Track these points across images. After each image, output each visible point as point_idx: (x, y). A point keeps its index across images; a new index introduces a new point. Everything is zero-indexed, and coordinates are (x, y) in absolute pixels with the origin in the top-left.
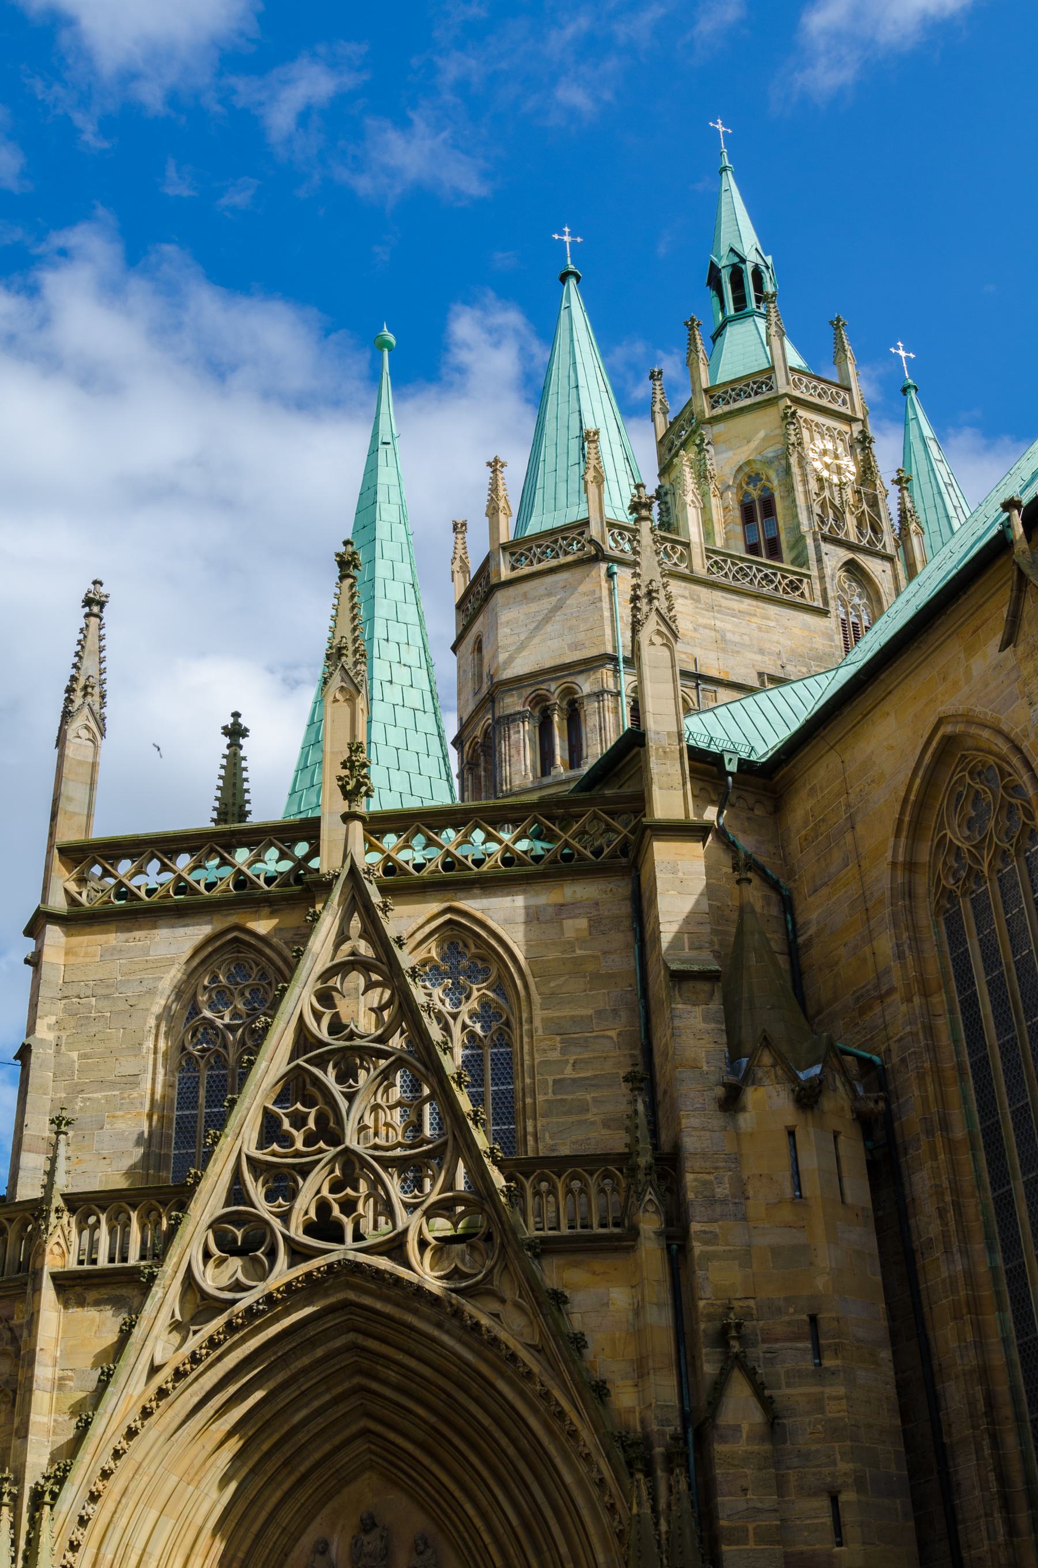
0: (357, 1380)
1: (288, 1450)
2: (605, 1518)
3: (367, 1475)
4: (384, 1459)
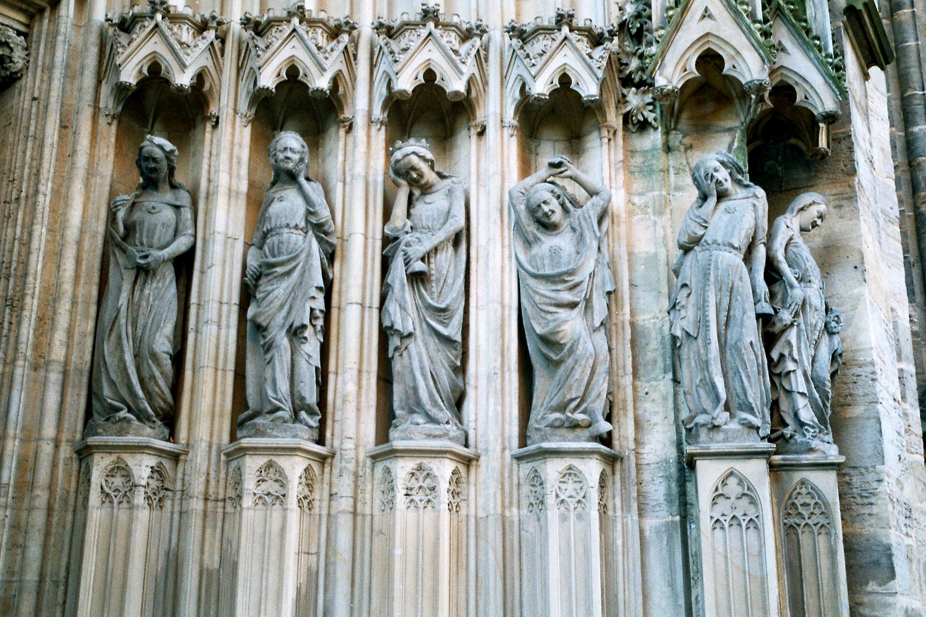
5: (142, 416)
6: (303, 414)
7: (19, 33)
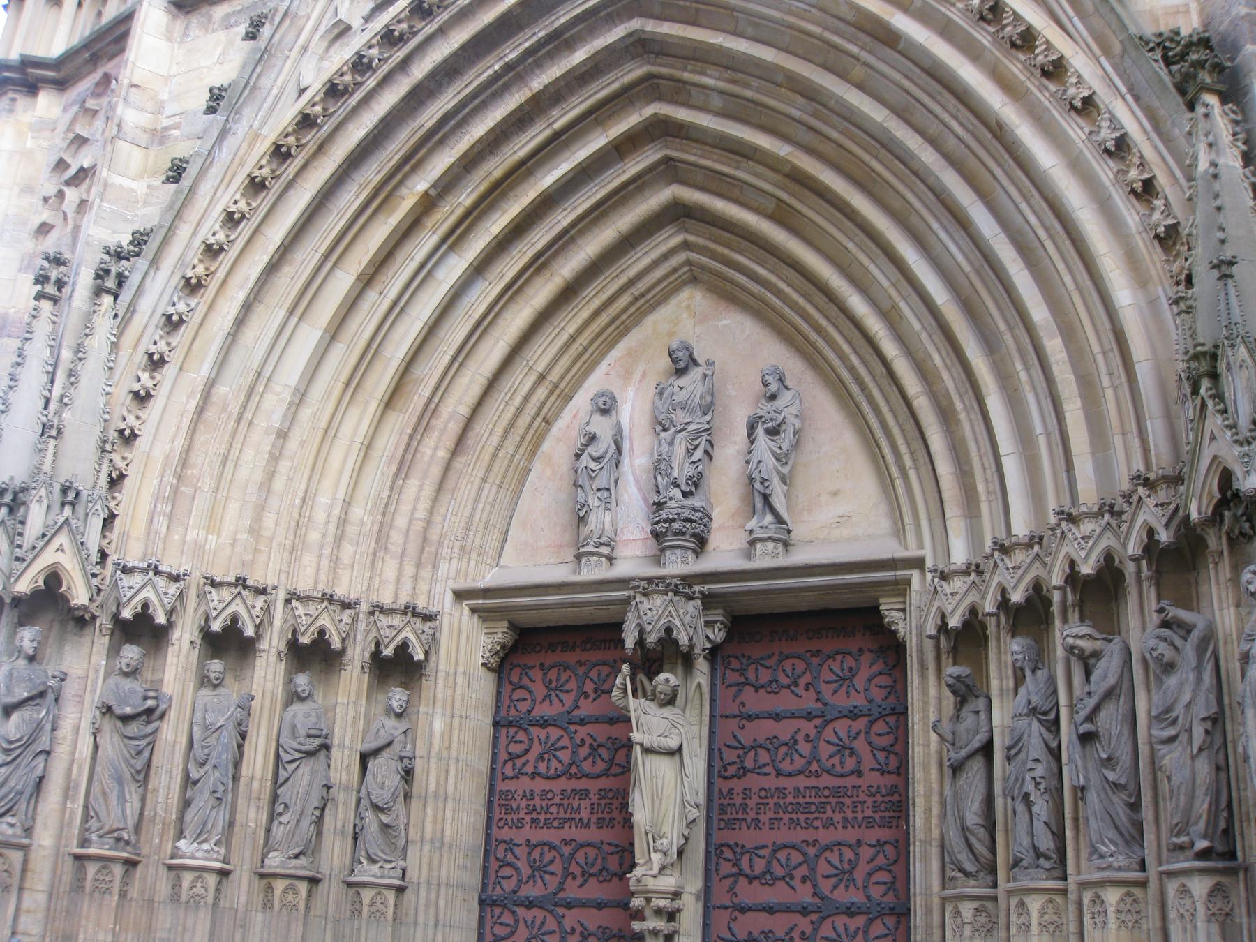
0: (650, 110)
1: (539, 238)
2: (1130, 214)
3: (685, 294)
4: (713, 256)
5: (967, 874)
6: (1042, 860)
7: (899, 610)
